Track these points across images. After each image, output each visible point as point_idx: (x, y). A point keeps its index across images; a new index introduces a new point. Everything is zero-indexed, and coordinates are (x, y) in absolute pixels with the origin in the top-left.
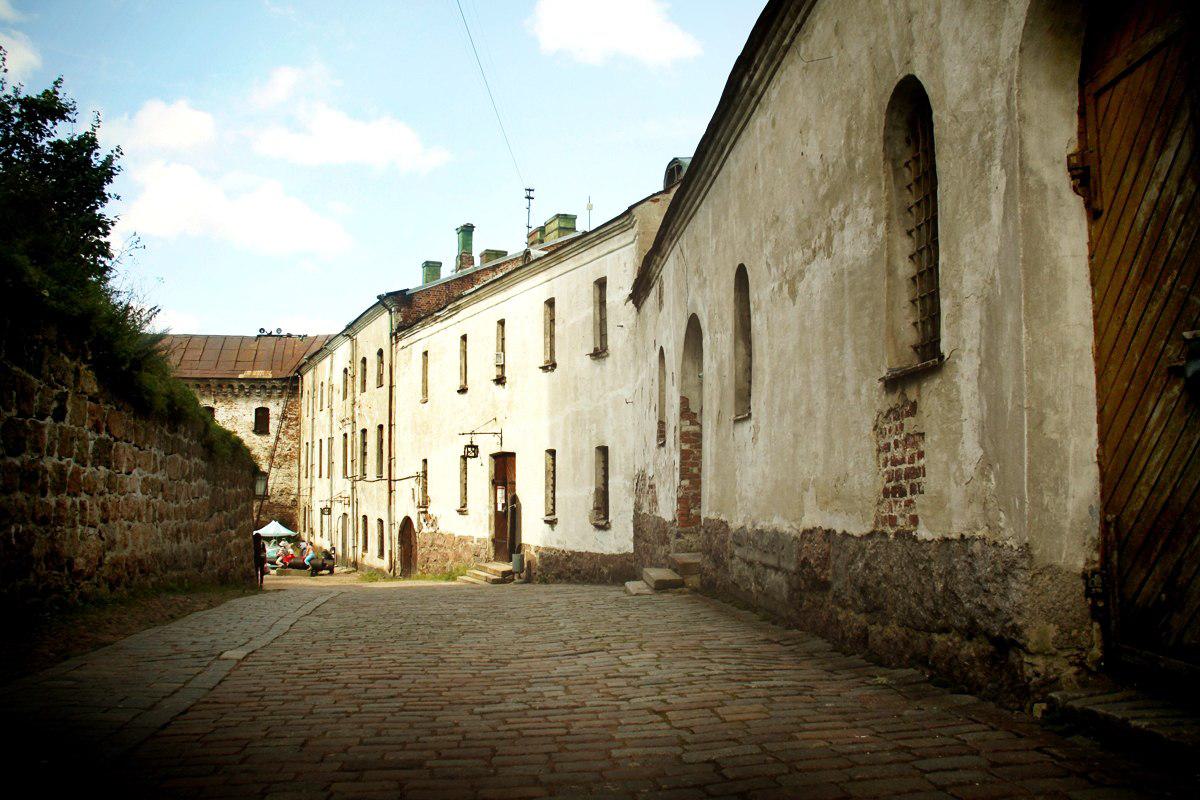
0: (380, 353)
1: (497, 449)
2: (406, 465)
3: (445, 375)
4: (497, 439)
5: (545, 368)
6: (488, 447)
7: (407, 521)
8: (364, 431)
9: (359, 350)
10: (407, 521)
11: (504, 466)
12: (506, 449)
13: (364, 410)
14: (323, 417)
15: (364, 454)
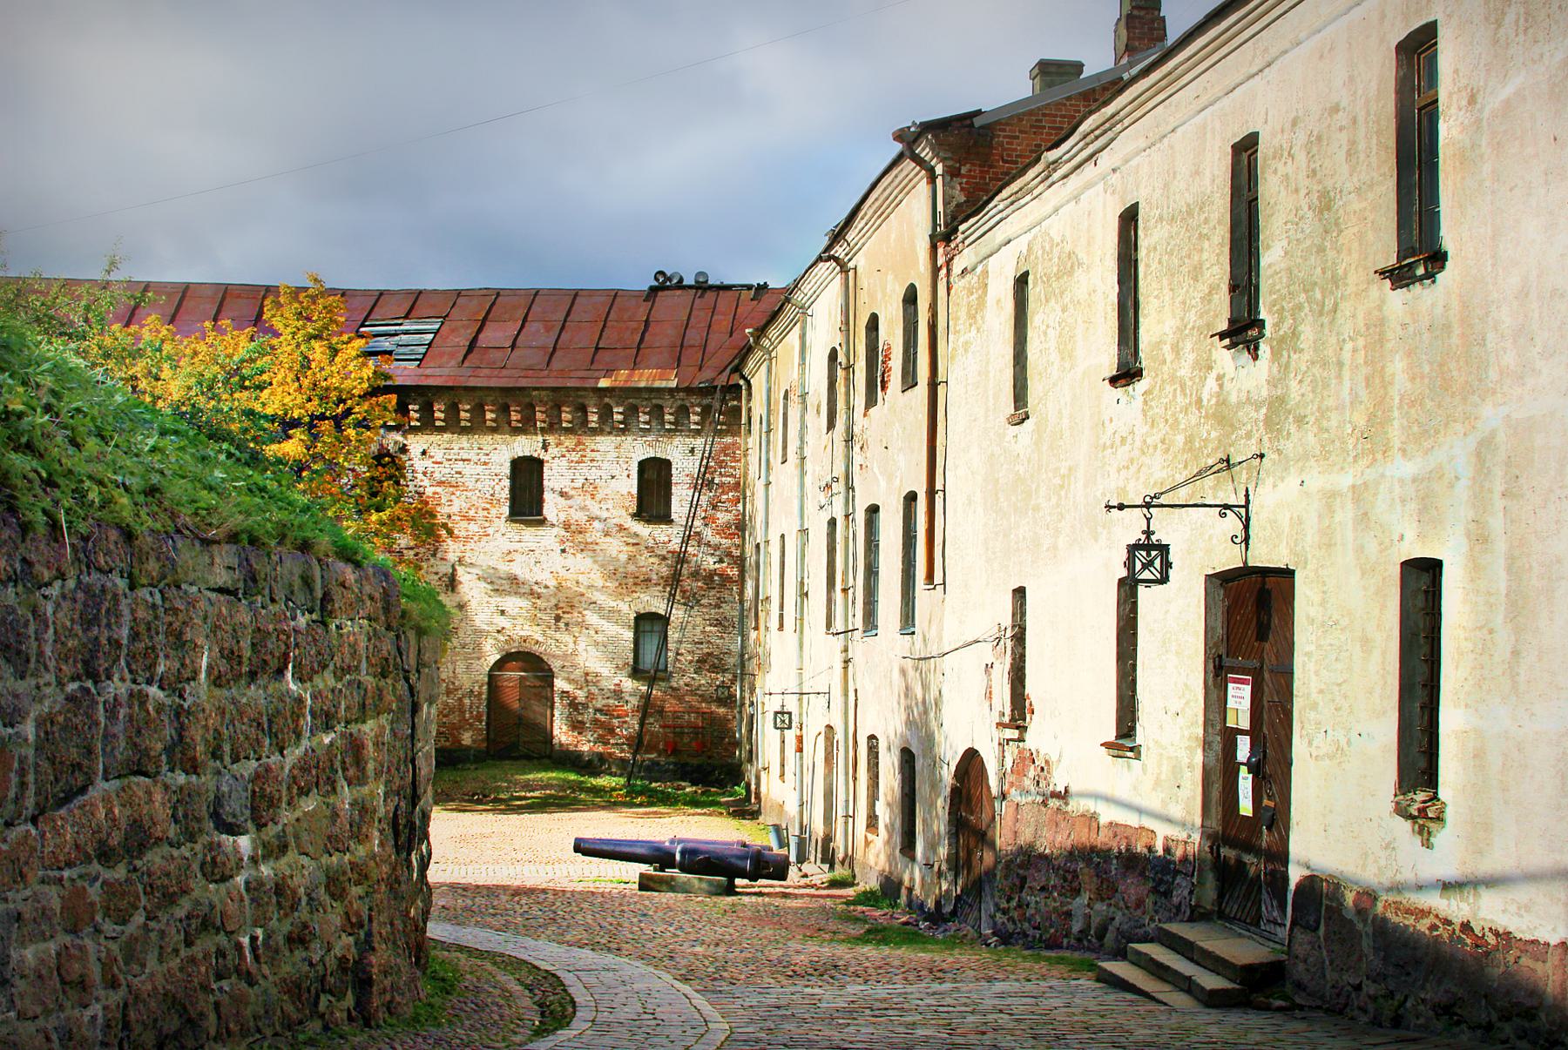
0: (910, 298)
1: (1230, 559)
2: (965, 610)
3: (1076, 332)
4: (1232, 524)
5: (1399, 276)
6: (1202, 547)
7: (971, 761)
8: (873, 510)
9: (863, 297)
10: (971, 761)
11: (1253, 614)
12: (1262, 556)
13: (874, 450)
14: (785, 476)
15: (872, 572)
